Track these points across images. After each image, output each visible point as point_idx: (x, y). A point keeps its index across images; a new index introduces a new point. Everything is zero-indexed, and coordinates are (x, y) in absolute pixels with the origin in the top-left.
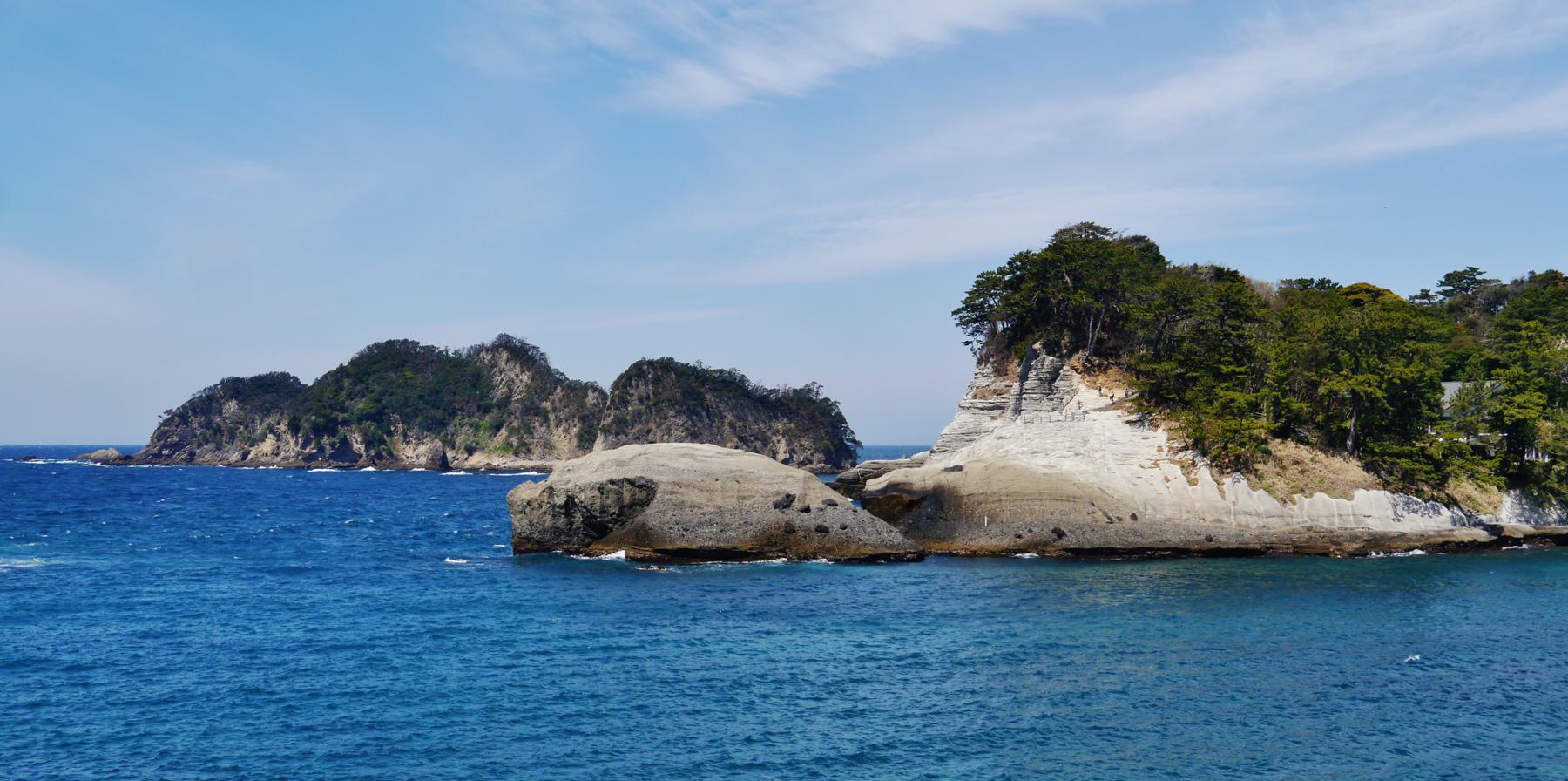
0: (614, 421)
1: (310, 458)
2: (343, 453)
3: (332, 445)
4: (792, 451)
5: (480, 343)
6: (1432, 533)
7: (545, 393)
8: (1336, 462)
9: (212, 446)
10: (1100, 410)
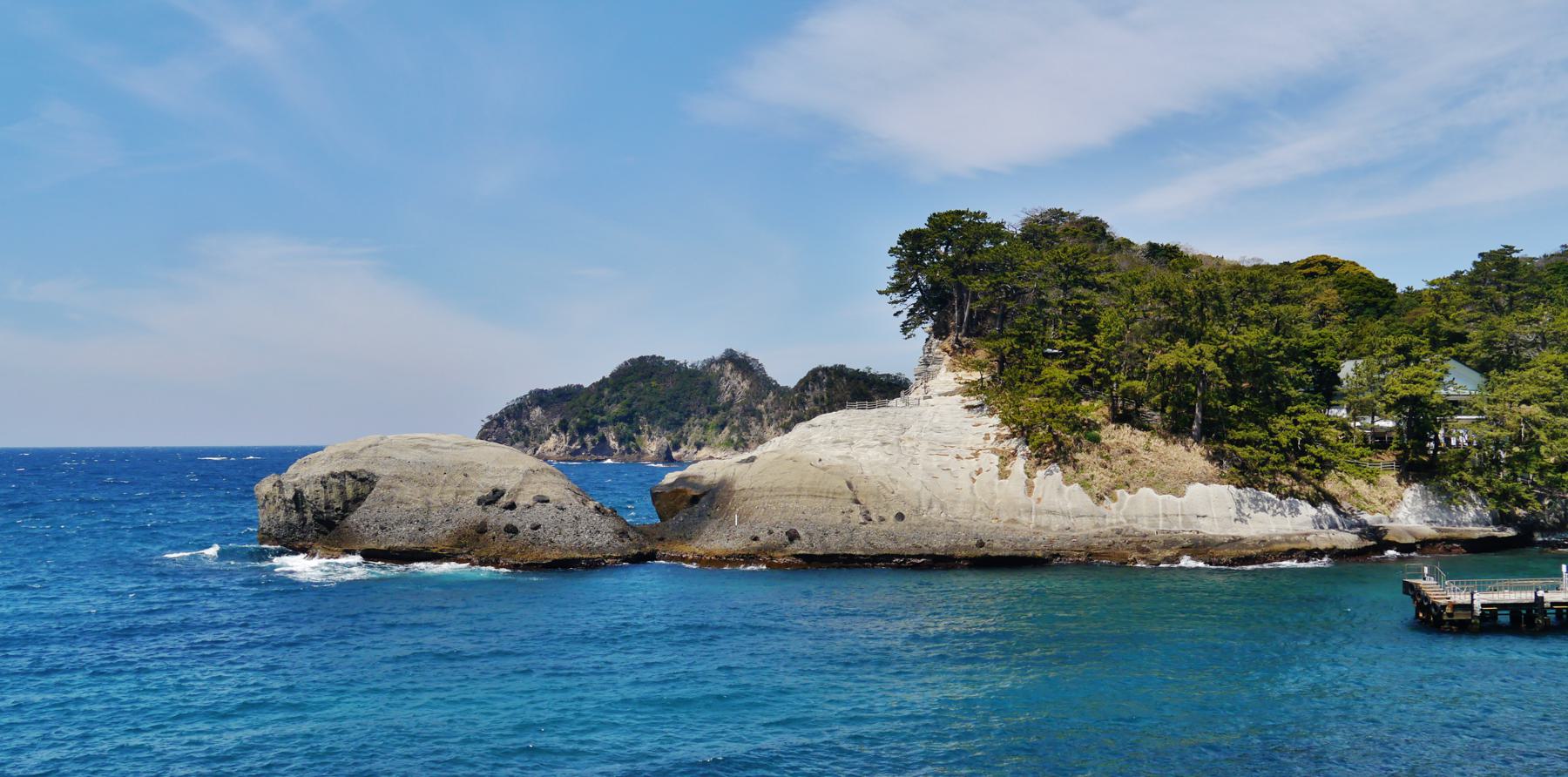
1: (576, 453)
2: (602, 448)
3: (593, 442)
5: (710, 357)
6: (1277, 538)
7: (760, 398)
8: (1177, 450)
10: (946, 394)
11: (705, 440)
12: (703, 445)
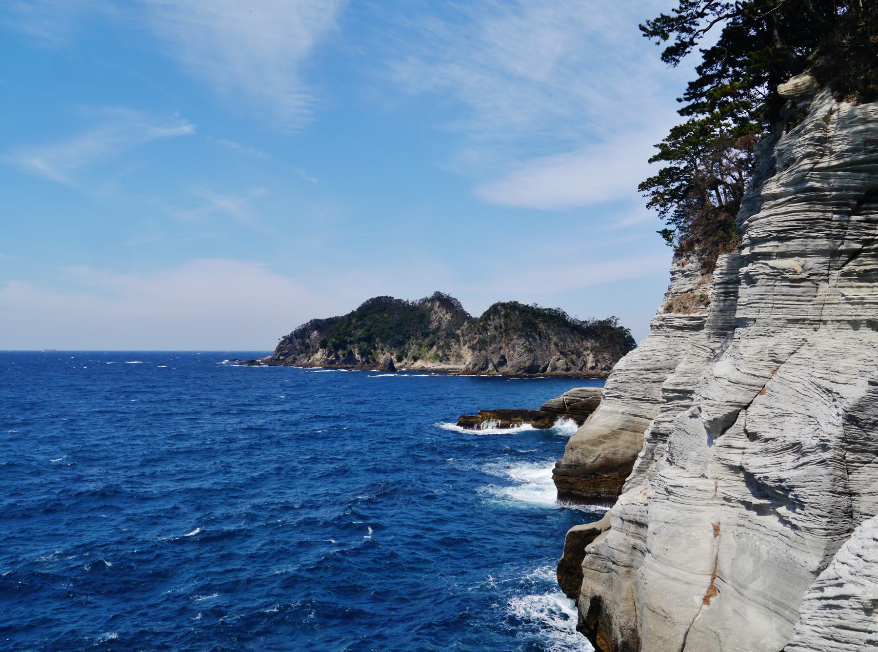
0: (478, 342)
1: (332, 362)
2: (350, 359)
3: (344, 355)
4: (597, 361)
7: (458, 325)
9: (304, 355)
11: (420, 355)
12: (418, 358)
